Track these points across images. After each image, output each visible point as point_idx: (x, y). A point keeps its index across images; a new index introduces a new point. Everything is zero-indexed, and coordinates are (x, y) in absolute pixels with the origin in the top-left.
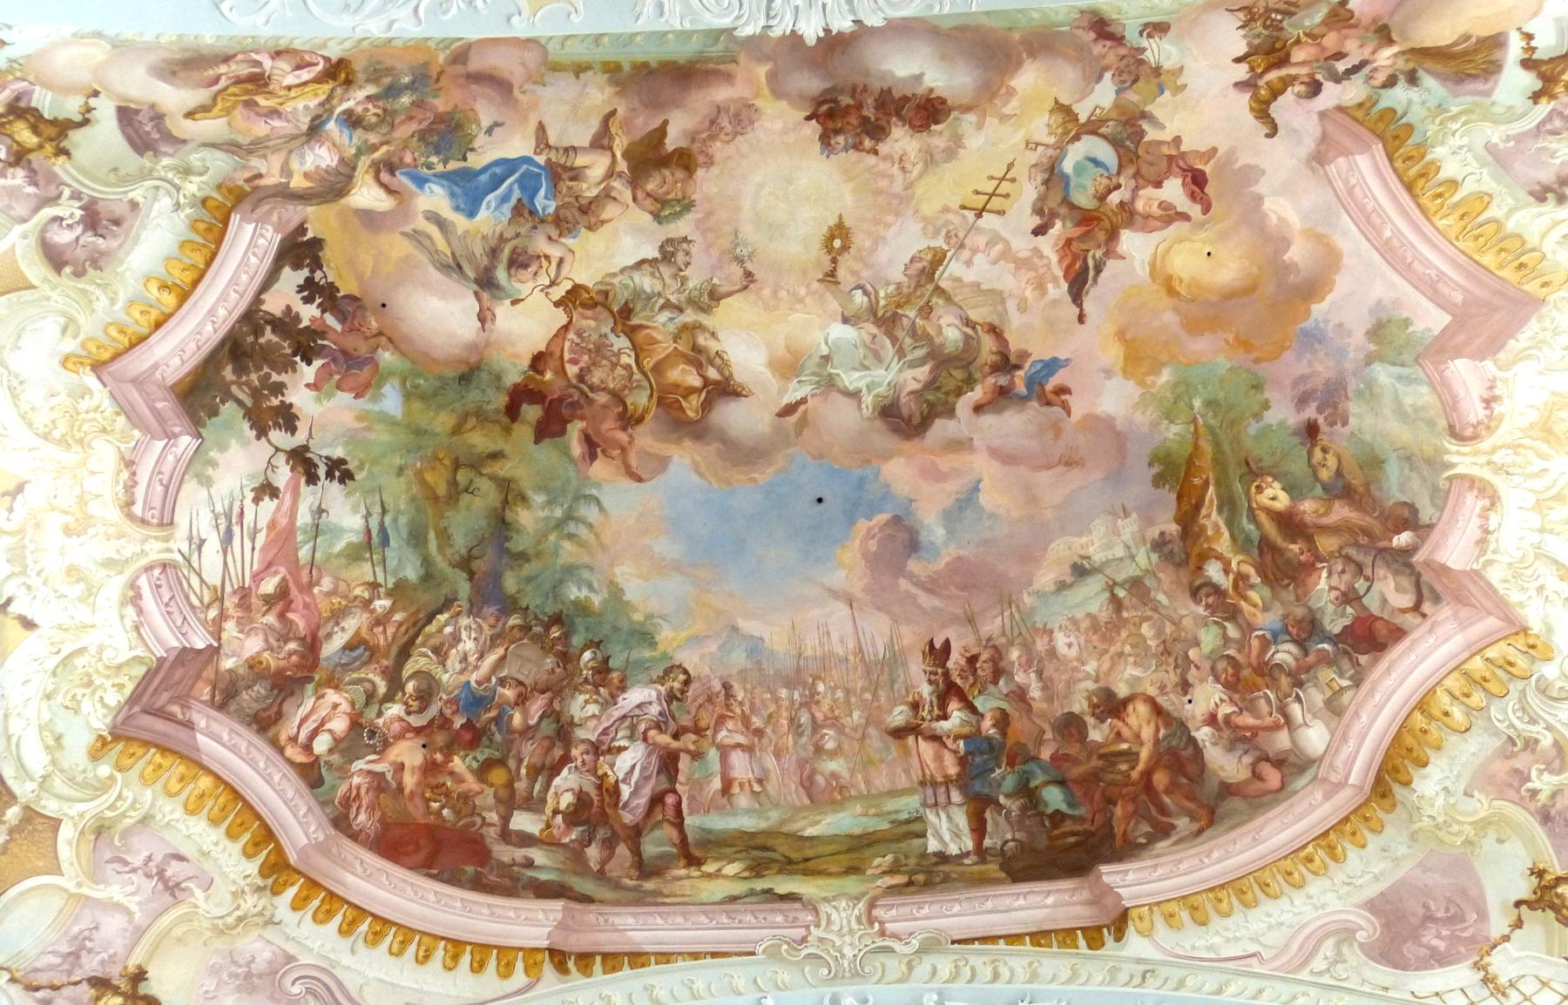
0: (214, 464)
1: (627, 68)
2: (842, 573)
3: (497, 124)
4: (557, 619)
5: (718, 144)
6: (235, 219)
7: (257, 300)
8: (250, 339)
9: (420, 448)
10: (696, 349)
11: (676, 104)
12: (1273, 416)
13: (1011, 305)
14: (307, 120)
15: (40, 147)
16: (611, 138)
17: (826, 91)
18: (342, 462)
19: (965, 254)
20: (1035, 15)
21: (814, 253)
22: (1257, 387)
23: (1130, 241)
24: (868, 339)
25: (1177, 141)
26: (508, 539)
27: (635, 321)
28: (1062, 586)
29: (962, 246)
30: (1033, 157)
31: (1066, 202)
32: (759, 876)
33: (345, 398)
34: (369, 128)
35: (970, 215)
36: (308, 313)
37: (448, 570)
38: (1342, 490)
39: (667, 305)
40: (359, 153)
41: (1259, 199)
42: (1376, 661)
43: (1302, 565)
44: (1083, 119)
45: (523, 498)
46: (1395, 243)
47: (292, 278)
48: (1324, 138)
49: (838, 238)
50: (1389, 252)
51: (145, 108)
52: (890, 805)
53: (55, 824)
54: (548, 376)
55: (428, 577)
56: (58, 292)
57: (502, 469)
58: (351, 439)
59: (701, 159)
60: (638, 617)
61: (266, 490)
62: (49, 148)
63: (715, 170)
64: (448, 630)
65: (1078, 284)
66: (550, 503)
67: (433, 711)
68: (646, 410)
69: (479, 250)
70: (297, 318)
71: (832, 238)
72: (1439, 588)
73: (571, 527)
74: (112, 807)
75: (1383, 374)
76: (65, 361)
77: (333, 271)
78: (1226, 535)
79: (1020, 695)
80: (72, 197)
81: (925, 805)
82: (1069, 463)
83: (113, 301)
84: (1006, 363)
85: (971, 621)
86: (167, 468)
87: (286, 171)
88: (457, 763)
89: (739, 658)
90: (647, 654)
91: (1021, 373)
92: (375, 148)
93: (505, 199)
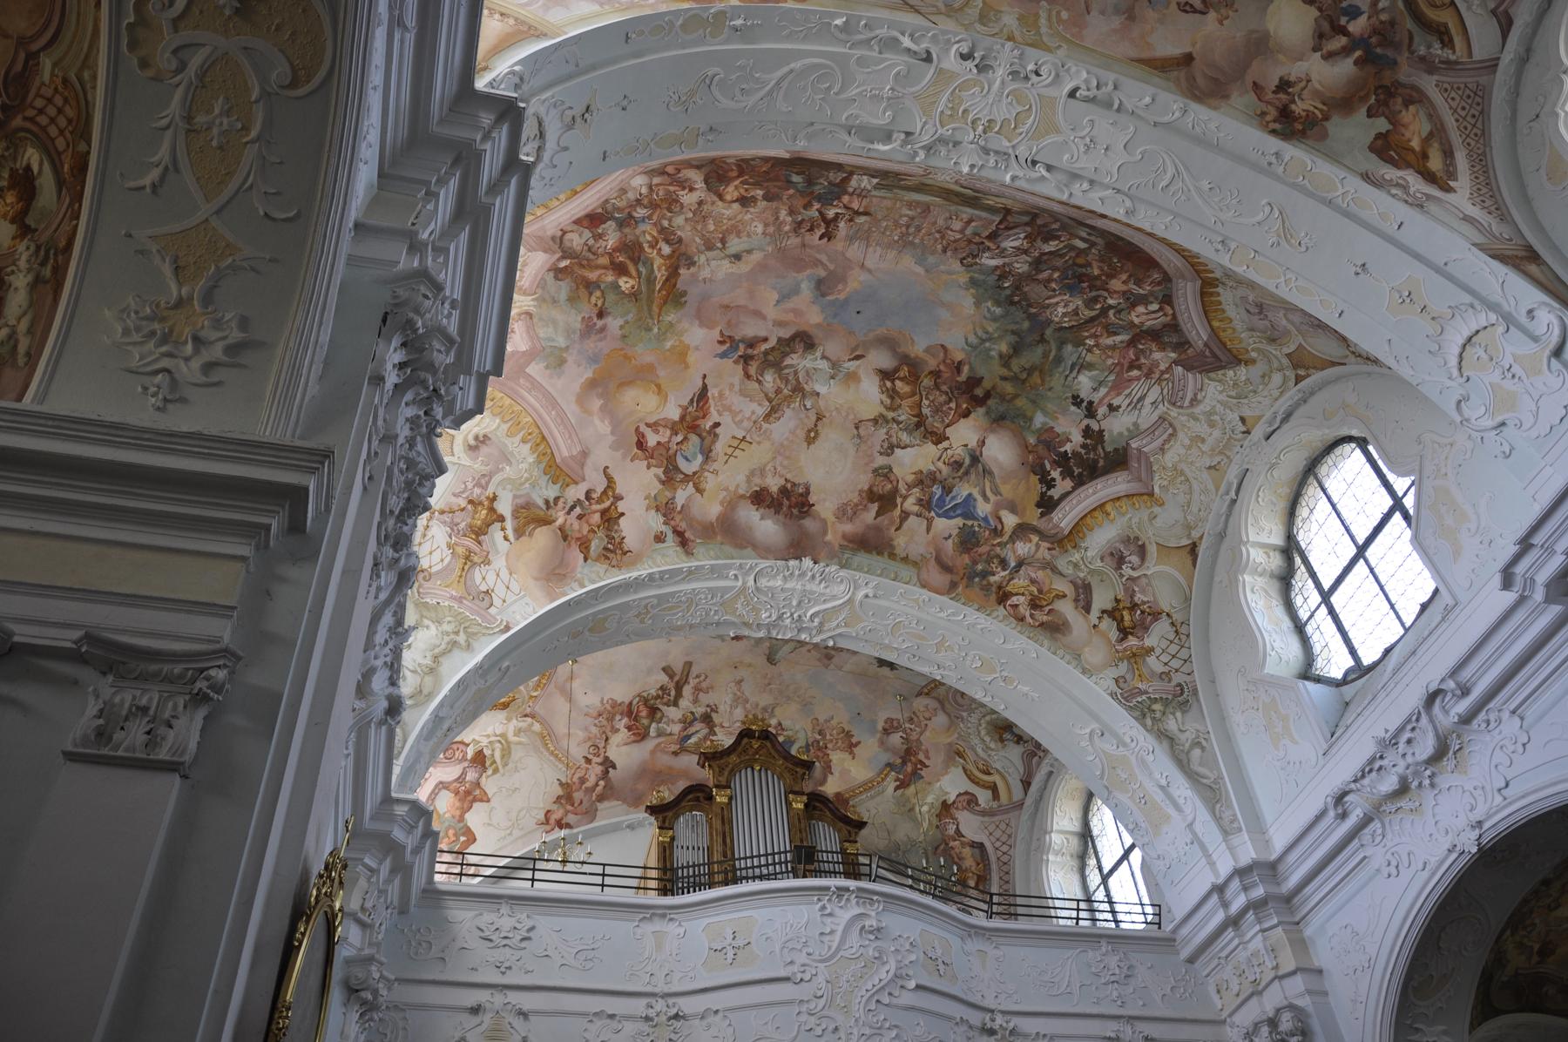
0: (1128, 430)
1: (886, 553)
2: (862, 278)
3: (946, 539)
4: (1012, 303)
5: (855, 501)
6: (1066, 532)
7: (1074, 489)
8: (1085, 473)
9: (1037, 395)
10: (892, 398)
11: (868, 527)
12: (620, 322)
13: (737, 388)
14: (1021, 572)
15: (1124, 608)
16: (900, 516)
17: (804, 518)
18: (1073, 404)
19: (754, 418)
20: (712, 553)
21: (824, 431)
22: (624, 337)
23: (674, 414)
24: (810, 382)
25: (648, 467)
26: (1017, 342)
27: (916, 419)
28: (749, 252)
29: (755, 422)
30: (715, 466)
31: (702, 439)
33: (1058, 430)
34: (998, 556)
35: (748, 439)
36: (1055, 474)
37: (1052, 342)
38: (590, 286)
39: (899, 423)
40: (1007, 543)
41: (613, 433)
42: (595, 209)
43: (620, 251)
44: (691, 483)
45: (1001, 356)
46: (550, 408)
47: (1055, 493)
48: (582, 465)
49: (811, 437)
50: (552, 403)
51: (1080, 609)
53: (1289, 355)
54: (965, 406)
55: (1062, 344)
56: (1149, 536)
57: (1005, 372)
58: (1065, 411)
59: (864, 495)
60: (972, 291)
61: (1112, 408)
62: (1121, 606)
63: (859, 487)
64: (1066, 319)
65: (703, 395)
66: (990, 350)
67: (1094, 294)
68: (926, 376)
69: (973, 476)
70: (1061, 473)
71: (814, 438)
72: (551, 243)
73: (984, 336)
74: (1260, 342)
75: (561, 342)
76: (1163, 504)
77: (1037, 487)
78: (655, 266)
79: (791, 212)
80: (1123, 576)
82: (727, 307)
83: (1130, 519)
84: (746, 359)
85: (804, 245)
86: (1148, 439)
87: (1038, 546)
88: (1096, 272)
89: (931, 259)
90: (976, 275)
91: (740, 353)
92: (999, 544)
93: (953, 498)
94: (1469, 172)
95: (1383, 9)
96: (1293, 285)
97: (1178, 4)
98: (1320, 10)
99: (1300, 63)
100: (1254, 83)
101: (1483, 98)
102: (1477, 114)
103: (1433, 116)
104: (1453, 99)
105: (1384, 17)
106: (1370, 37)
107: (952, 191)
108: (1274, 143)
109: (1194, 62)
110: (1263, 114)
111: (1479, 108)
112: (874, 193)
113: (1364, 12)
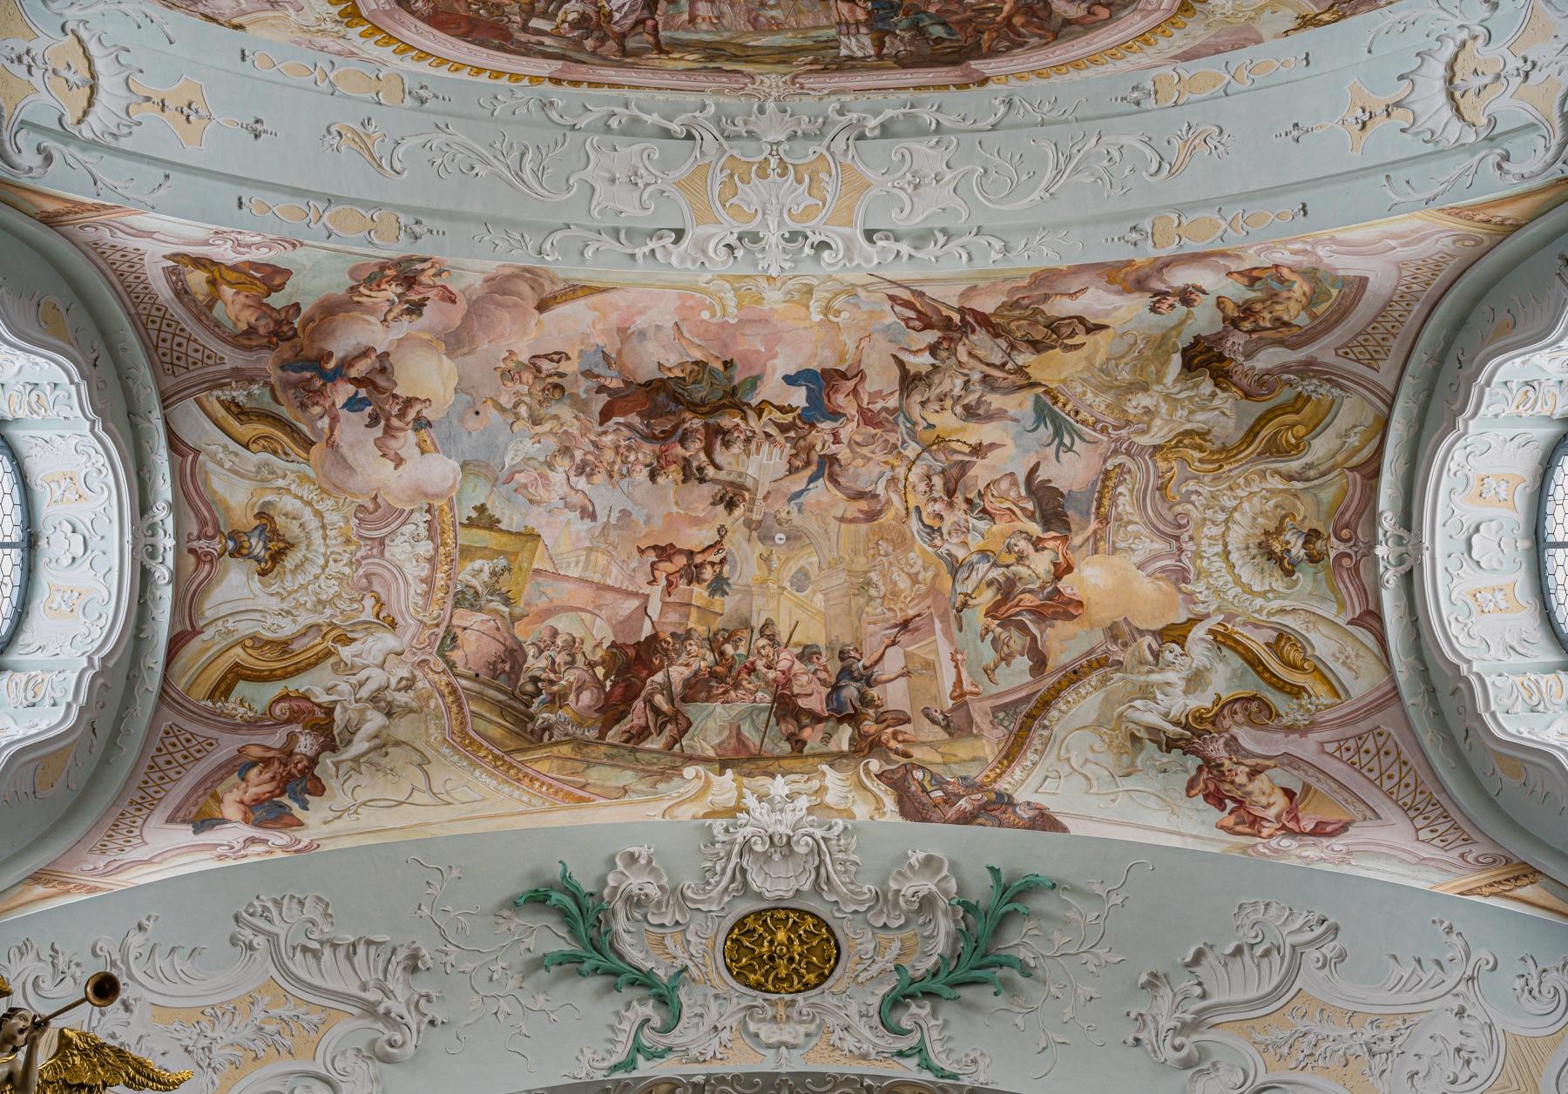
32: (711, 61)
52: (813, 34)
81: (840, 33)
94: (150, 280)
95: (321, 417)
96: (316, 74)
97: (568, 358)
98: (395, 396)
99: (401, 336)
100: (454, 302)
101: (162, 363)
102: (161, 344)
103: (216, 328)
104: (197, 351)
105: (317, 410)
106: (324, 385)
107: (746, 62)
108: (419, 250)
109: (536, 303)
110: (439, 274)
111: (161, 351)
112: (833, 32)
113: (343, 407)
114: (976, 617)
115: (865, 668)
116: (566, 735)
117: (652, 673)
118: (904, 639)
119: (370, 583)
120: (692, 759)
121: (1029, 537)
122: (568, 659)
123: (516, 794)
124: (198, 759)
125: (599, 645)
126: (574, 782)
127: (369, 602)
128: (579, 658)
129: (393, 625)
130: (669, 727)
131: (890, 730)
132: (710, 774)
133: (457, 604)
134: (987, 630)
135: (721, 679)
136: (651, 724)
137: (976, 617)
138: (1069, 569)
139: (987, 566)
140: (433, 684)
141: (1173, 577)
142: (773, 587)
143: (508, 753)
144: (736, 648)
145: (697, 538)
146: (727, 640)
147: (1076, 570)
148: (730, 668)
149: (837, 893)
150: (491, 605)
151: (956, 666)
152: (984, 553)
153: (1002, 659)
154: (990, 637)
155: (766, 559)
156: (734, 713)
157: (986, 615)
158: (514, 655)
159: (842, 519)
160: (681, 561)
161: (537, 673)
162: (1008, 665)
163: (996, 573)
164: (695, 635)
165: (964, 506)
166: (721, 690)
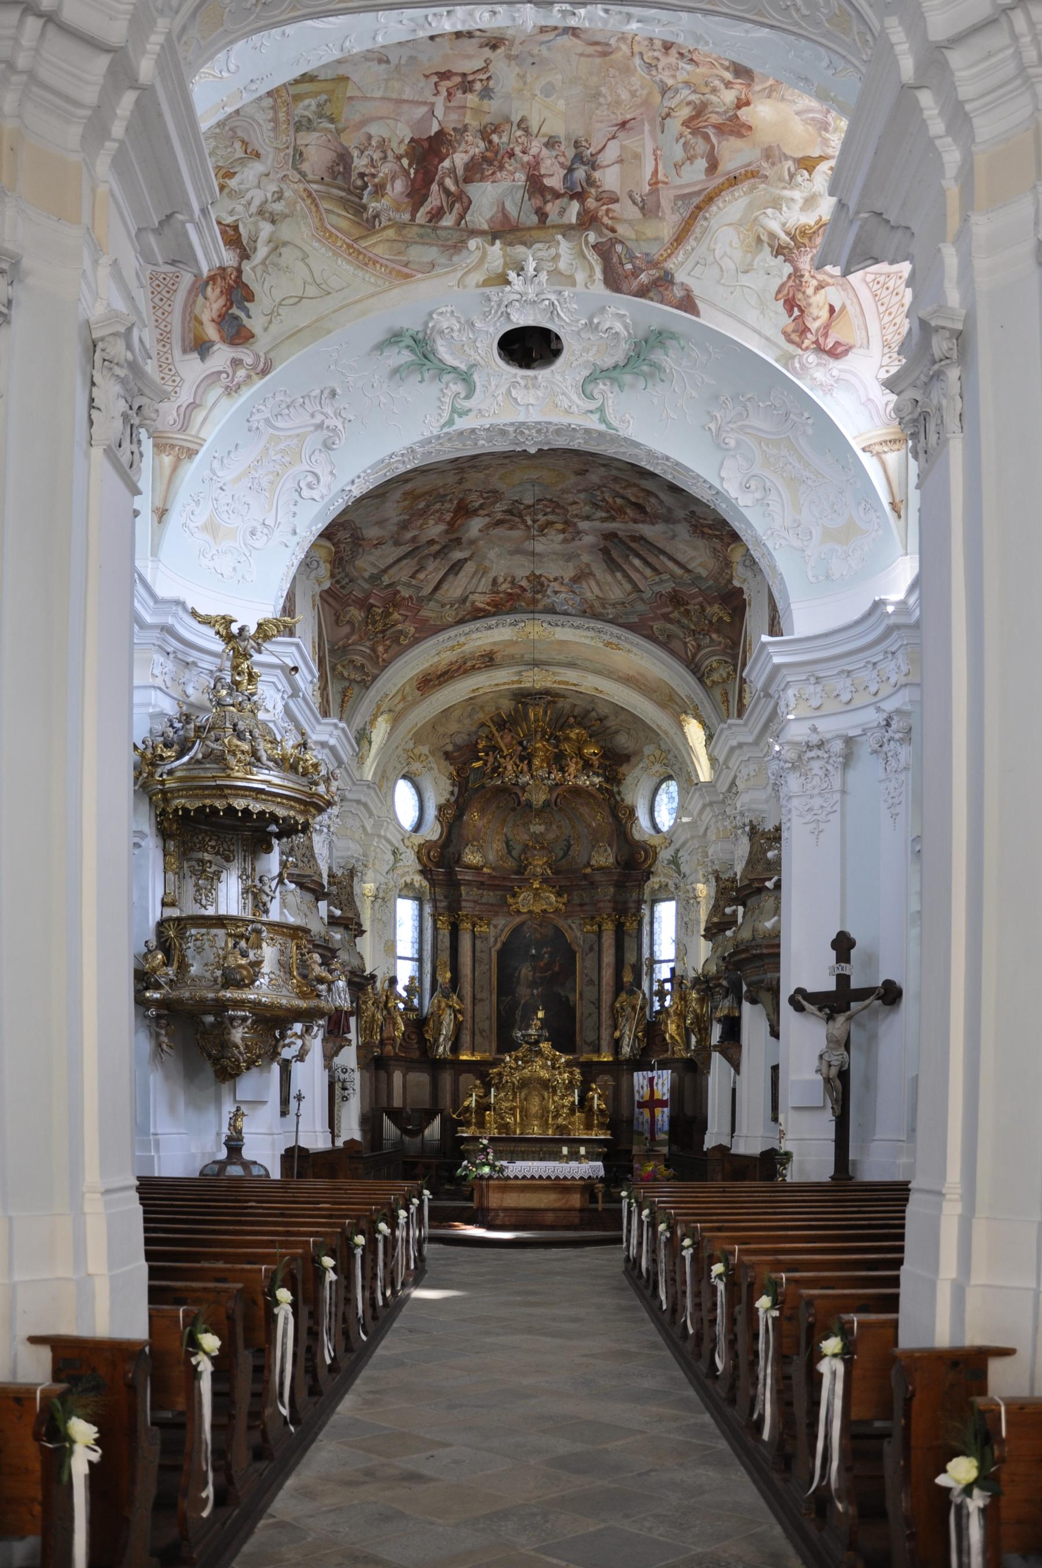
114: (675, 125)
115: (592, 155)
116: (390, 220)
117: (442, 160)
118: (621, 135)
119: (235, 132)
120: (474, 233)
121: (722, 80)
122: (382, 155)
123: (367, 276)
124: (175, 291)
125: (402, 141)
126: (400, 261)
127: (238, 145)
128: (390, 153)
129: (258, 155)
130: (457, 205)
131: (604, 207)
132: (486, 245)
133: (298, 130)
134: (681, 136)
135: (490, 163)
136: (445, 204)
137: (675, 125)
138: (748, 103)
139: (688, 92)
140: (295, 191)
141: (819, 126)
142: (527, 94)
143: (356, 240)
144: (500, 137)
145: (468, 66)
146: (494, 132)
147: (752, 106)
148: (497, 153)
149: (564, 321)
150: (321, 125)
151: (656, 160)
152: (687, 83)
153: (688, 159)
154: (682, 140)
155: (522, 77)
156: (500, 191)
157: (683, 124)
158: (343, 158)
159: (582, 55)
160: (458, 79)
161: (362, 170)
162: (692, 164)
163: (693, 97)
164: (469, 127)
165: (677, 56)
166: (490, 172)
